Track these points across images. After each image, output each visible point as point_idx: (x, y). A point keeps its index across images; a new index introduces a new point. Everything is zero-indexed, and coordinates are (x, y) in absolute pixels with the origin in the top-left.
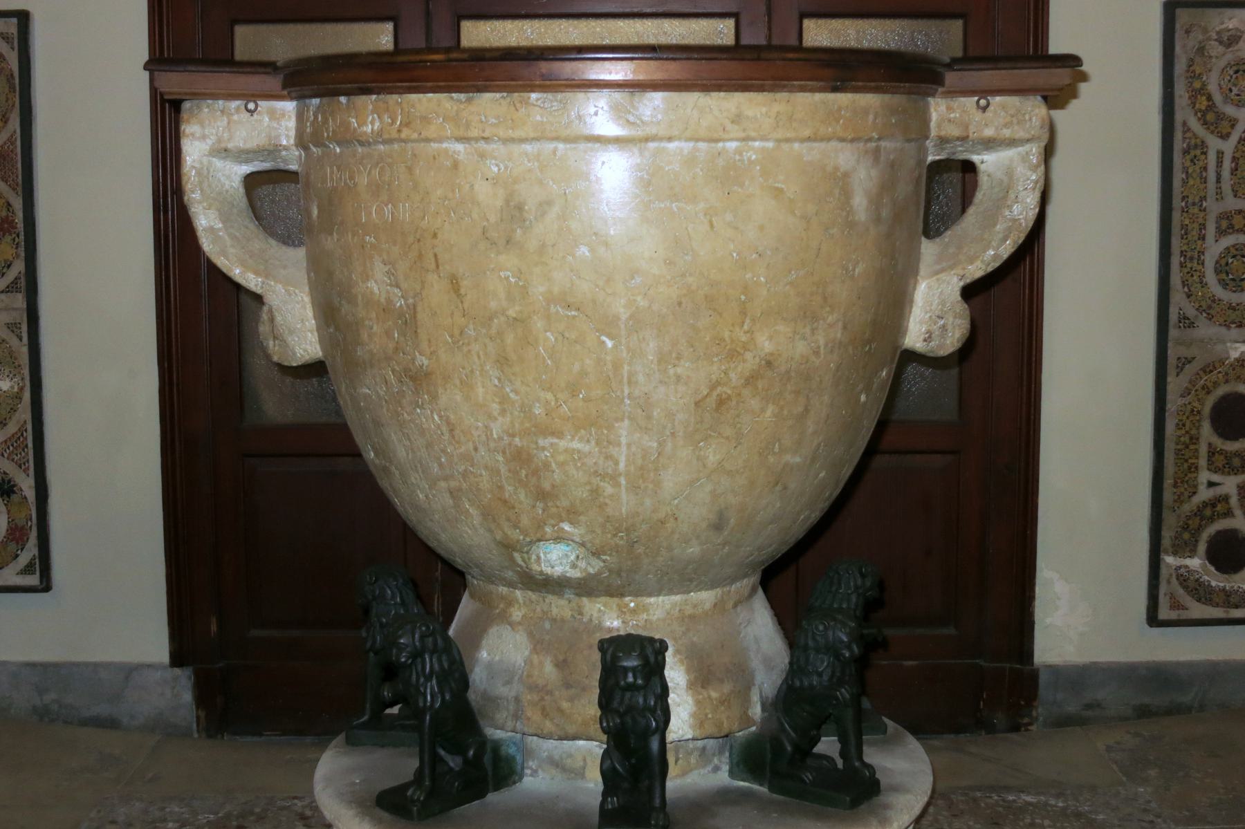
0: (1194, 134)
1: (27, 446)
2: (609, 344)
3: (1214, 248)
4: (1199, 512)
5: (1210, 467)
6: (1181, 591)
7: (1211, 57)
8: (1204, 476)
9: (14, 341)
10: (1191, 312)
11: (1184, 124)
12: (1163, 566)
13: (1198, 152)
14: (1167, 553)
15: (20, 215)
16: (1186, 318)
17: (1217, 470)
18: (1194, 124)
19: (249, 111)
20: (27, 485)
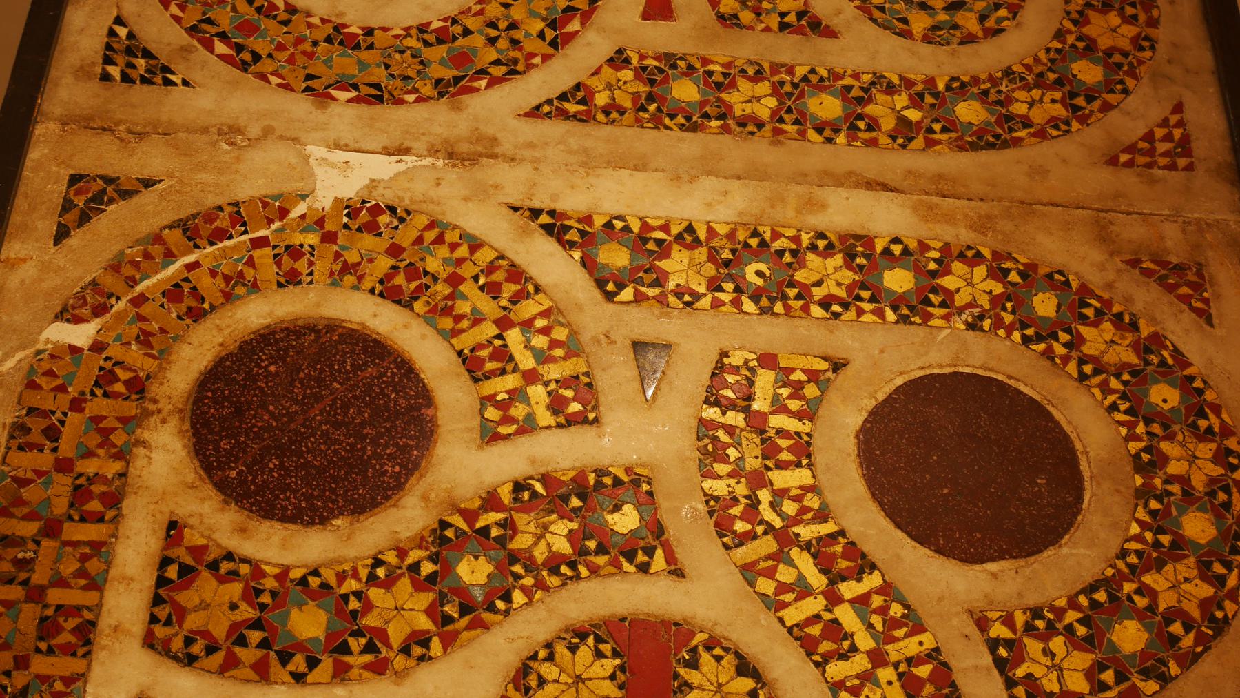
5: (160, 631)
16: (134, 48)
17: (197, 649)
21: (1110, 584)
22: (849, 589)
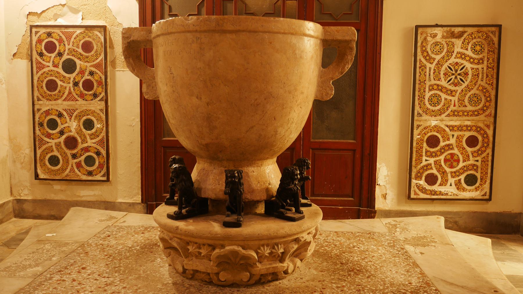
0: (423, 63)
1: (104, 142)
3: (428, 95)
4: (423, 167)
6: (417, 190)
7: (428, 41)
8: (424, 158)
9: (101, 114)
10: (421, 112)
11: (420, 60)
12: (412, 182)
13: (424, 68)
14: (413, 179)
15: (104, 80)
18: (423, 60)
20: (104, 152)
21: (479, 149)
22: (464, 150)
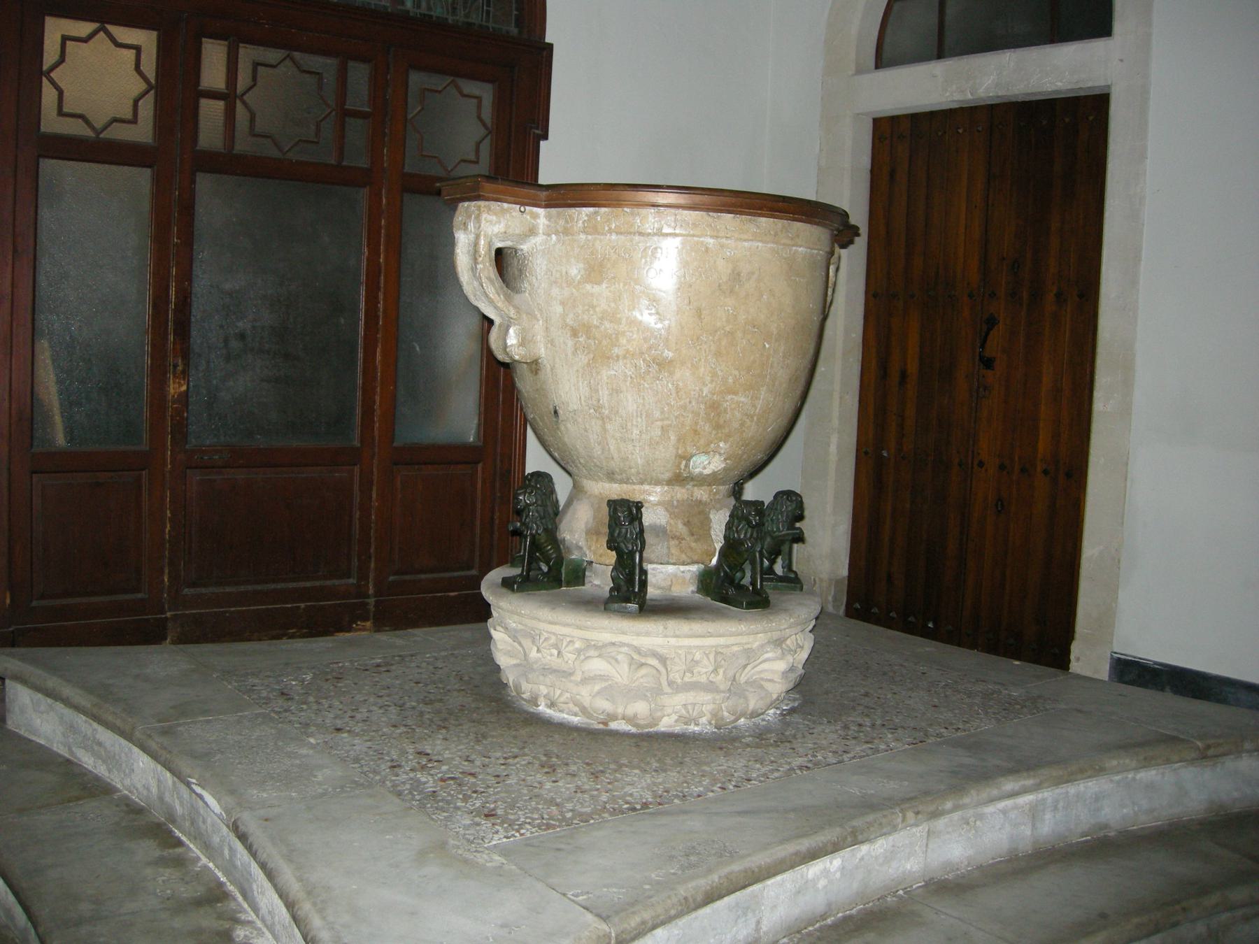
2: (767, 346)
19: (521, 212)
